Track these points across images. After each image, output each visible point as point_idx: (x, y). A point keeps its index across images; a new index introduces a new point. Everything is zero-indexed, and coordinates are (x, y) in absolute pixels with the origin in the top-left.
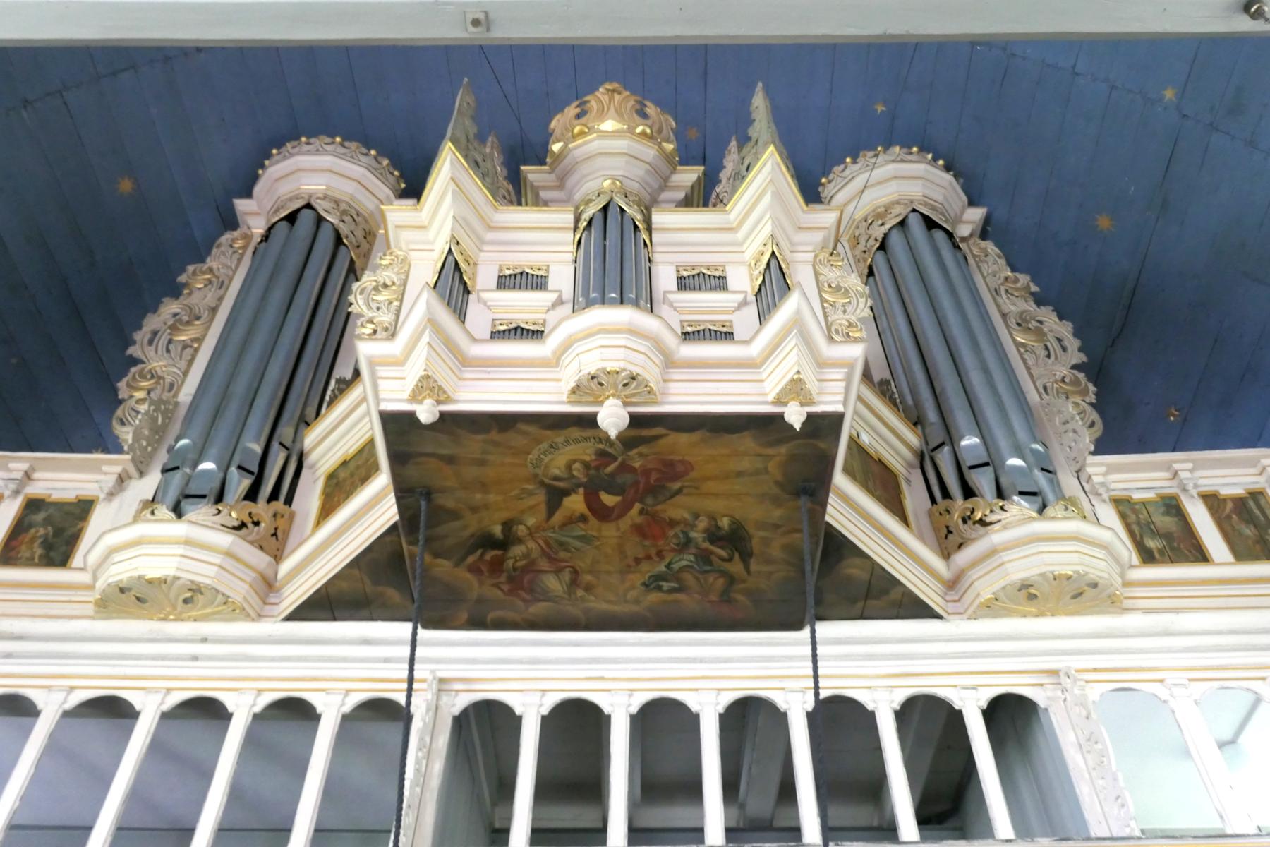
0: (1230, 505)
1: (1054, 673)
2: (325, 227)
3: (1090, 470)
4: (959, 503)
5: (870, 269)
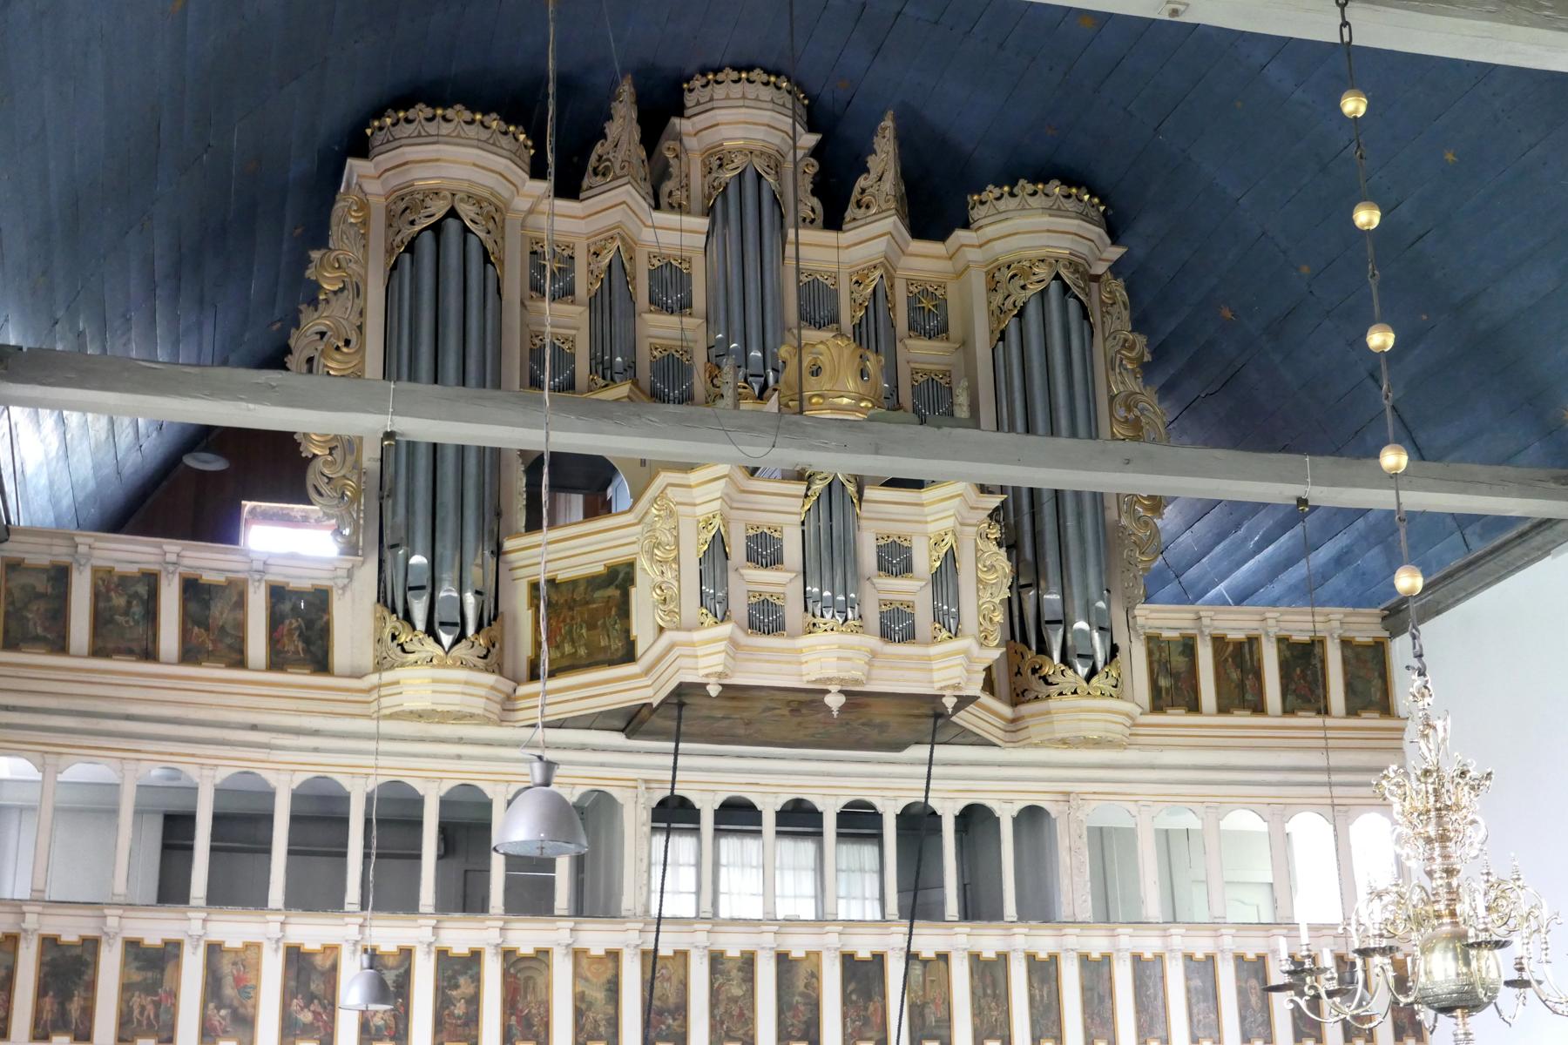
0: (1231, 648)
1: (1068, 794)
2: (472, 240)
3: (1136, 612)
4: (1031, 655)
5: (1003, 333)
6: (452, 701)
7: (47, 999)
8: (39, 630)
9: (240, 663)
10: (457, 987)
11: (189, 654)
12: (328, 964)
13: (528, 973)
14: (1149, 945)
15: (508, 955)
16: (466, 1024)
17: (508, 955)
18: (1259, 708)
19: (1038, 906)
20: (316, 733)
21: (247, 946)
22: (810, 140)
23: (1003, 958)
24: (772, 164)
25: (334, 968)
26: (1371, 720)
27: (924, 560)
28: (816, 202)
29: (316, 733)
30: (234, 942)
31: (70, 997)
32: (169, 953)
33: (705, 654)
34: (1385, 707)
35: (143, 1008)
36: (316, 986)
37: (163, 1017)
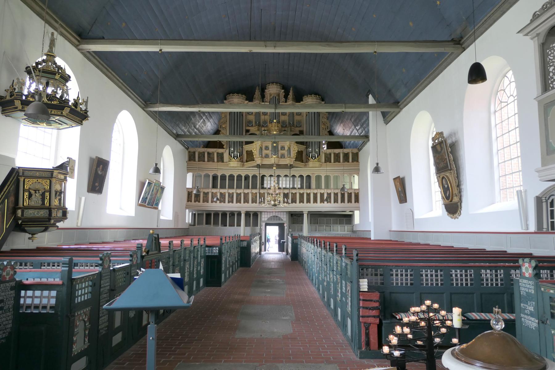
6: (236, 166)
9: (214, 162)
11: (208, 161)
14: (322, 191)
15: (244, 193)
17: (244, 193)
18: (339, 162)
19: (309, 187)
23: (303, 193)
26: (355, 163)
27: (286, 148)
32: (208, 193)
33: (258, 161)
34: (357, 161)
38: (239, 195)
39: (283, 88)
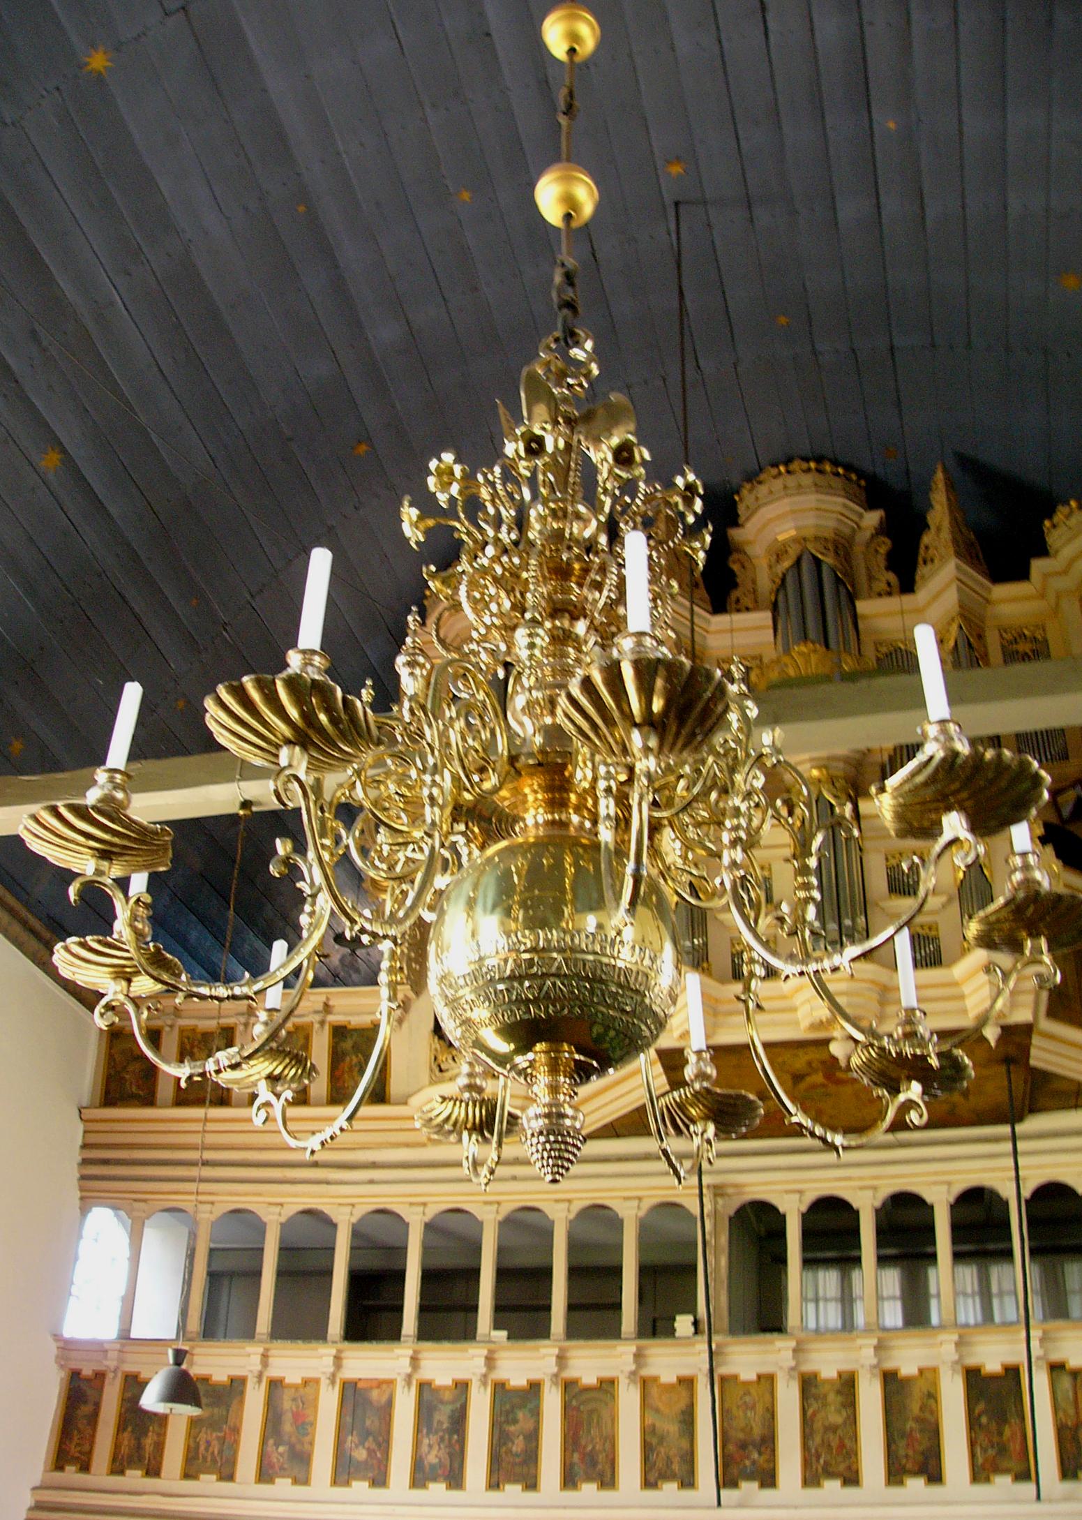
7: (126, 1435)
8: (134, 1089)
10: (515, 1421)
12: (384, 1399)
13: (591, 1406)
15: (569, 1387)
16: (524, 1463)
17: (569, 1387)
20: (374, 1165)
21: (306, 1382)
22: (873, 518)
24: (830, 546)
25: (390, 1404)
28: (892, 577)
29: (374, 1165)
30: (293, 1377)
31: (145, 1434)
35: (208, 1443)
36: (371, 1422)
37: (226, 1453)
38: (515, 1404)
39: (872, 491)
